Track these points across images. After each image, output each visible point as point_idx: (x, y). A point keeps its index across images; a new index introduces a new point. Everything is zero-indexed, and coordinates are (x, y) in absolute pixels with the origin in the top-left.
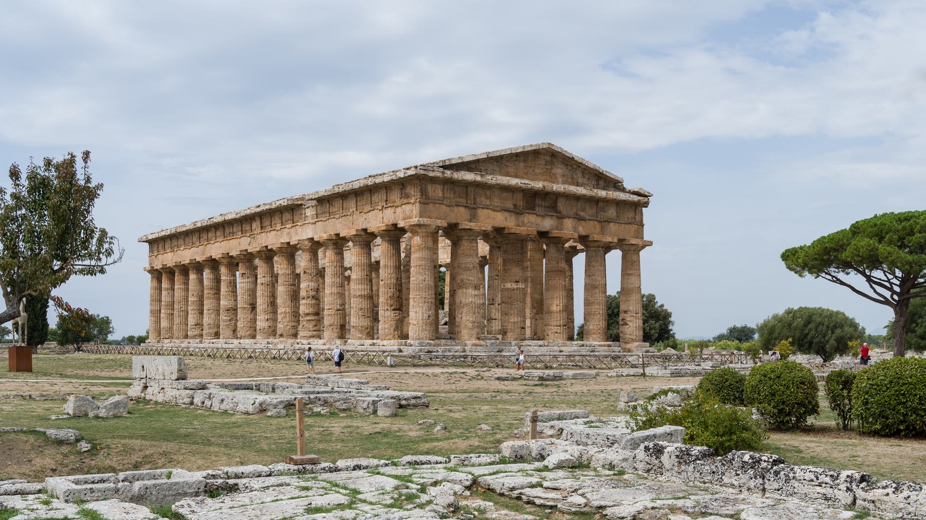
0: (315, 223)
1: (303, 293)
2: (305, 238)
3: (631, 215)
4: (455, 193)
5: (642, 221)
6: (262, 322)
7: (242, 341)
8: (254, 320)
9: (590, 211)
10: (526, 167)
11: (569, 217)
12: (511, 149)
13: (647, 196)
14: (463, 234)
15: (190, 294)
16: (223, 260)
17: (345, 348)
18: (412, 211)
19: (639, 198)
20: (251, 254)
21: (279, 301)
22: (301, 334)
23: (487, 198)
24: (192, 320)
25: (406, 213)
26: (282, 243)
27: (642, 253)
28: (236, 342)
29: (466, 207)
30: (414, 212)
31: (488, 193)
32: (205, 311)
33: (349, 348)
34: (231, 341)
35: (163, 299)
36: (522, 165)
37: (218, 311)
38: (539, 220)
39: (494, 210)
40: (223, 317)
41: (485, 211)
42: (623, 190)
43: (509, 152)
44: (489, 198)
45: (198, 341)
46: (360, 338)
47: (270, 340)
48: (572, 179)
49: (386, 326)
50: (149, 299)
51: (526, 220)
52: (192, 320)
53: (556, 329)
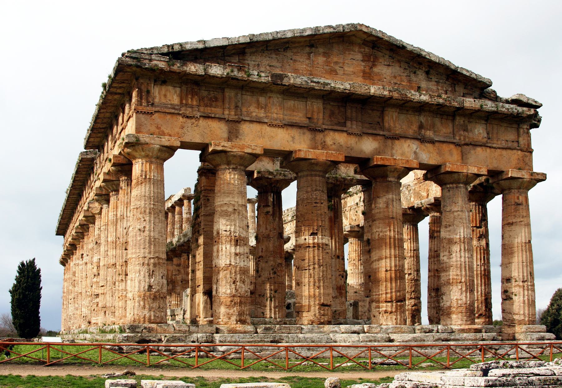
3: (511, 136)
4: (201, 99)
5: (529, 144)
9: (444, 130)
10: (327, 63)
11: (406, 138)
12: (293, 31)
14: (218, 159)
19: (520, 109)
23: (259, 106)
27: (533, 193)
31: (262, 100)
36: (321, 60)
38: (352, 141)
41: (256, 127)
42: (495, 98)
44: (265, 107)
48: (410, 81)
53: (384, 306)
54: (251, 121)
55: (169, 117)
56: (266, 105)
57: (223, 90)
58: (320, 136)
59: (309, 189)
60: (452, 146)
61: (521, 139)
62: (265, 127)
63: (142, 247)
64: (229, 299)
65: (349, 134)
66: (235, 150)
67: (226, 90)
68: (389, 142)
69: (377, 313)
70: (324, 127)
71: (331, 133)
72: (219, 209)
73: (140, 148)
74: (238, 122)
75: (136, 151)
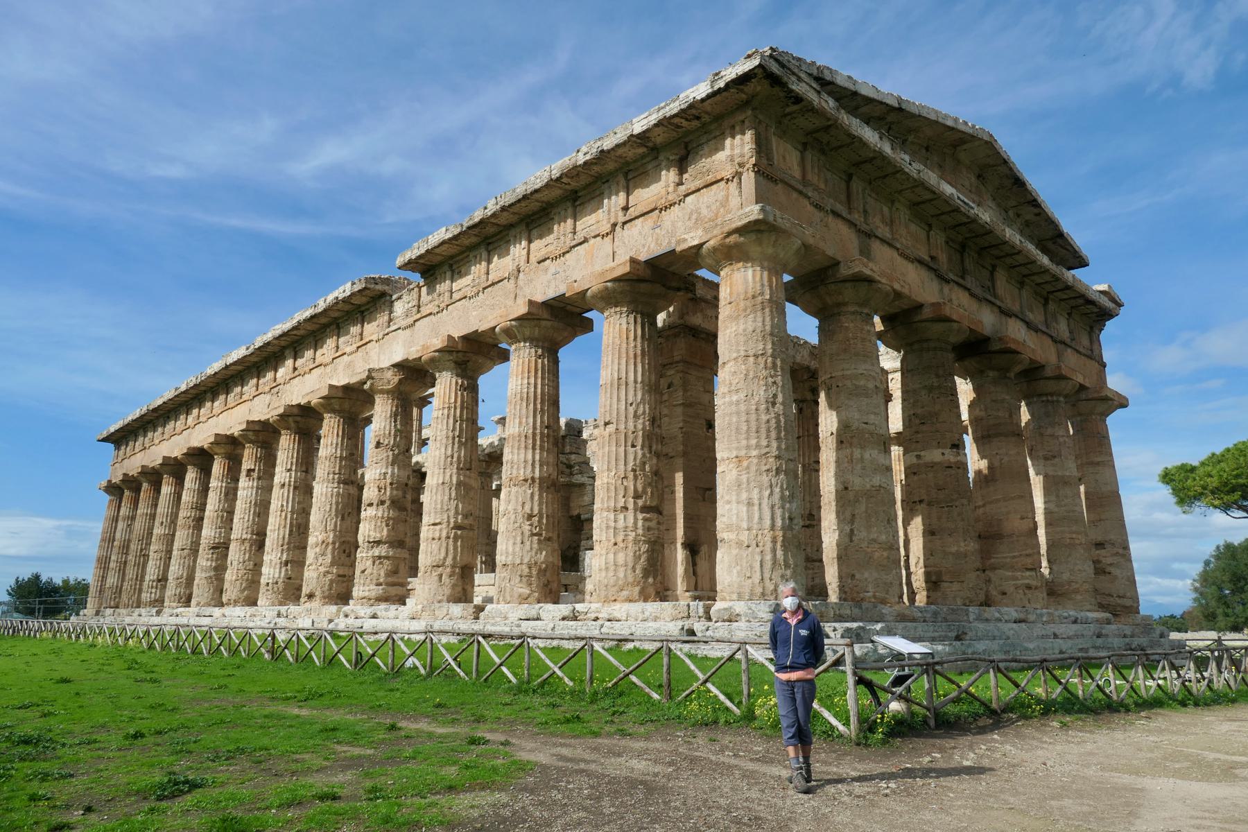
0: (412, 325)
1: (369, 494)
2: (386, 363)
6: (272, 568)
7: (227, 610)
8: (258, 565)
13: (1120, 305)
14: (848, 293)
15: (157, 523)
16: (217, 449)
17: (477, 627)
18: (725, 203)
20: (265, 425)
21: (315, 518)
22: (357, 592)
24: (152, 572)
25: (710, 201)
26: (331, 387)
28: (217, 612)
29: (852, 224)
30: (734, 201)
31: (885, 209)
32: (175, 553)
33: (490, 629)
34: (209, 610)
35: (118, 535)
37: (194, 550)
39: (904, 256)
40: (204, 561)
43: (933, 117)
45: (154, 610)
46: (524, 599)
47: (283, 609)
49: (621, 558)
50: (100, 537)
51: (954, 297)
52: (152, 572)
54: (883, 241)
55: (795, 195)
56: (892, 221)
57: (850, 176)
58: (946, 289)
59: (941, 372)
60: (1049, 340)
61: (1095, 347)
62: (895, 254)
63: (773, 434)
64: (885, 554)
65: (972, 295)
66: (884, 281)
67: (854, 178)
68: (1004, 318)
69: (1012, 589)
70: (951, 276)
71: (956, 288)
72: (848, 383)
73: (773, 238)
74: (870, 235)
75: (760, 244)
